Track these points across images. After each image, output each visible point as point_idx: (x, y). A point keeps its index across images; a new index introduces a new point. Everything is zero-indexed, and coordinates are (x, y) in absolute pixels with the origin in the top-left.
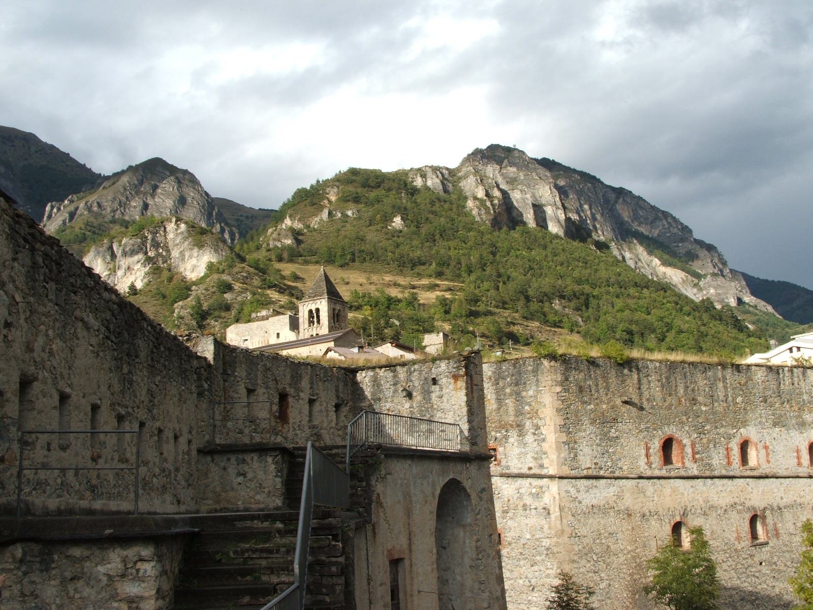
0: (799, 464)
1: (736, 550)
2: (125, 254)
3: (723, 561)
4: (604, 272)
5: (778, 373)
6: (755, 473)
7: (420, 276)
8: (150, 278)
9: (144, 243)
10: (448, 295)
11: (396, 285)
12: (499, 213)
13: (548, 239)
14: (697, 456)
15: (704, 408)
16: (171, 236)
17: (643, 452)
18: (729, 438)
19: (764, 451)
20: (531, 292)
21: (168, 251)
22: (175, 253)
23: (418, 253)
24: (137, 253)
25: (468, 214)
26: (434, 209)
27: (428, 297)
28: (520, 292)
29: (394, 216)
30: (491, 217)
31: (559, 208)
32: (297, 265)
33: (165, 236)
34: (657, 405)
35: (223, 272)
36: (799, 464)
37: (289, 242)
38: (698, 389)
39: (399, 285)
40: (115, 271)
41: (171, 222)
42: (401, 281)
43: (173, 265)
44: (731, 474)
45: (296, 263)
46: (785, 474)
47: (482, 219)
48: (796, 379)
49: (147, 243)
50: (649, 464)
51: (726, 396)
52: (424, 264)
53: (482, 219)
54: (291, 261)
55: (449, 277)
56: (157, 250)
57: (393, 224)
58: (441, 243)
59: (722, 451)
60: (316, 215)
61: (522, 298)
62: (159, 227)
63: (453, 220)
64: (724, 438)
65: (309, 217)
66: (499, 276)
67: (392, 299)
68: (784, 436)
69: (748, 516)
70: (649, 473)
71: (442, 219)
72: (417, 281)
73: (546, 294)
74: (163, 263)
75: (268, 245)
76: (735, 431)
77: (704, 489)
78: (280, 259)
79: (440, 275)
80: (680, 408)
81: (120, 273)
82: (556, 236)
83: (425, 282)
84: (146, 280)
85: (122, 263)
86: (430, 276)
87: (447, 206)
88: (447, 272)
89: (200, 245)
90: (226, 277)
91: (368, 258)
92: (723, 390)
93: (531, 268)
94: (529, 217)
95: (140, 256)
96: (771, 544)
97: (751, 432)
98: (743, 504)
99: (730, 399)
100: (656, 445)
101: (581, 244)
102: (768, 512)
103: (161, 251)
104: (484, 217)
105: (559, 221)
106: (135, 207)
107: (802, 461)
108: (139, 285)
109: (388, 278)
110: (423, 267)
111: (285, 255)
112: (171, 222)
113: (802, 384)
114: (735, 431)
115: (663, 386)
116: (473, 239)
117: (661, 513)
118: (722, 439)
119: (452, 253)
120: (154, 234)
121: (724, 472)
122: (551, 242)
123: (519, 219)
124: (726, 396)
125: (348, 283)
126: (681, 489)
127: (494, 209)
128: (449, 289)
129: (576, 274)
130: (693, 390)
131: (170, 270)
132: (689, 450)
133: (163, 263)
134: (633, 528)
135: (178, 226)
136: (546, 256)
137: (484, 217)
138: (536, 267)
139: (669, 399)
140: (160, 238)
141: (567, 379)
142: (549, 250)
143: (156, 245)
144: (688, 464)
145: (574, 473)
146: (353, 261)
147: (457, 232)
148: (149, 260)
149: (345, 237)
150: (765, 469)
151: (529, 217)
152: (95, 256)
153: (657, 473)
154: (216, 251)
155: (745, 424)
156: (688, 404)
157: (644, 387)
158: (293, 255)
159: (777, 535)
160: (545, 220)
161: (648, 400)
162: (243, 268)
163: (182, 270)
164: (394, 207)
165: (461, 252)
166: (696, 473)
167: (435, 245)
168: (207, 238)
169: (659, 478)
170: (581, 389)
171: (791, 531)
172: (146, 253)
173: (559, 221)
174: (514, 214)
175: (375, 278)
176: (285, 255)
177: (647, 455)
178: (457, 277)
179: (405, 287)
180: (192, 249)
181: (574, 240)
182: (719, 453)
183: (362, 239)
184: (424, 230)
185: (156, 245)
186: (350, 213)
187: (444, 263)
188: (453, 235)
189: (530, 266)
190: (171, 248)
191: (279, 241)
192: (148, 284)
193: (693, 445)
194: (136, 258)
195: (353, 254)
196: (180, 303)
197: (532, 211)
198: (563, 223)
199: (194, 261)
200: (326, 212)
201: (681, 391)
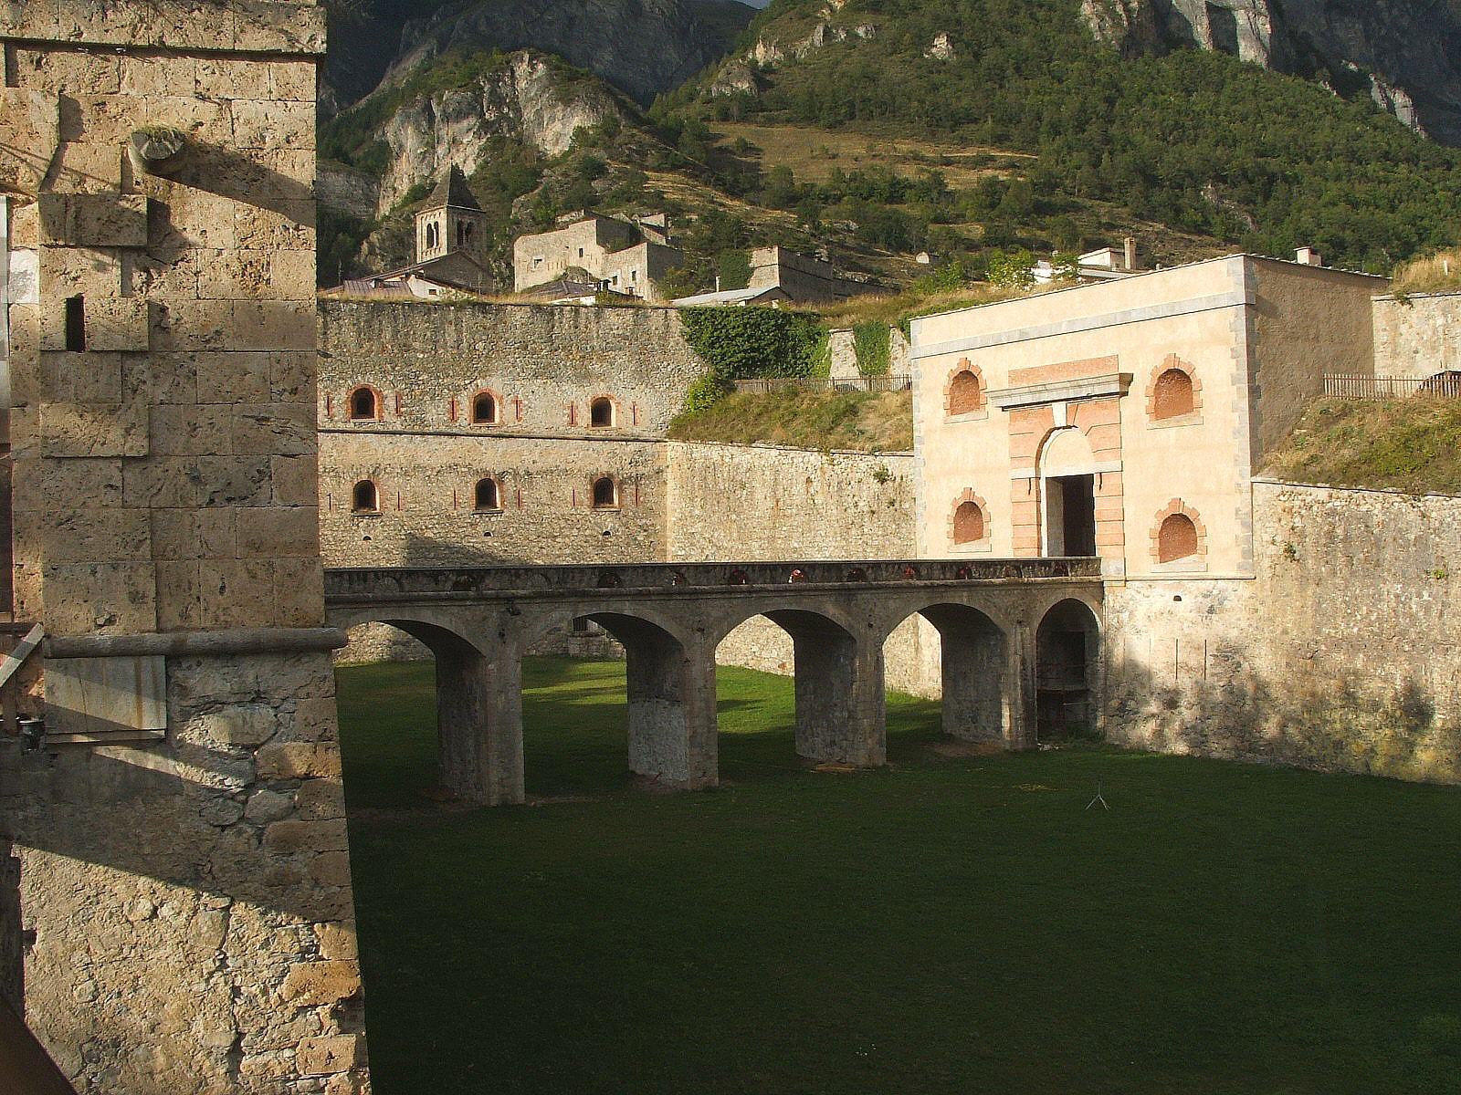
0: (572, 423)
1: (448, 517)
2: (447, 118)
3: (426, 528)
4: (1327, 131)
5: (552, 314)
6: (495, 432)
7: (964, 142)
8: (487, 157)
9: (478, 98)
10: (1003, 176)
11: (917, 158)
12: (1140, 25)
13: (1227, 73)
14: (403, 410)
16: (523, 84)
18: (457, 389)
19: (514, 406)
20: (1161, 172)
21: (518, 111)
22: (528, 114)
23: (965, 102)
24: (466, 116)
25: (1080, 29)
26: (1014, 20)
27: (961, 180)
28: (1135, 170)
29: (935, 37)
30: (1123, 33)
31: (1260, 14)
32: (753, 127)
33: (513, 85)
34: (349, 351)
35: (594, 145)
36: (572, 423)
37: (744, 86)
38: (414, 333)
39: (923, 159)
40: (433, 147)
41: (522, 61)
42: (928, 151)
43: (526, 133)
44: (454, 431)
45: (751, 122)
46: (545, 434)
47: (1105, 38)
48: (582, 321)
49: (482, 98)
50: (330, 417)
51: (459, 341)
52: (976, 121)
53: (1105, 38)
54: (743, 119)
55: (1016, 144)
56: (499, 109)
57: (934, 50)
58: (1014, 83)
59: (444, 406)
60: (806, 37)
61: (1140, 179)
62: (503, 70)
63: (1046, 40)
64: (449, 390)
65: (796, 40)
66: (1108, 140)
67: (898, 183)
68: (549, 388)
69: (473, 481)
71: (1025, 39)
72: (958, 151)
73: (1190, 174)
74: (509, 131)
75: (709, 91)
76: (467, 382)
77: (410, 446)
78: (725, 117)
79: (1000, 140)
81: (441, 150)
82: (1251, 67)
83: (971, 152)
84: (480, 161)
85: (443, 133)
86: (983, 142)
87: (1041, 14)
88: (1014, 131)
89: (567, 100)
90: (599, 154)
91: (876, 112)
93: (1177, 126)
94: (1201, 31)
95: (472, 121)
96: (506, 513)
97: (495, 385)
99: (465, 344)
101: (1301, 80)
103: (506, 110)
104: (1109, 33)
105: (1258, 38)
106: (551, 23)
107: (578, 419)
108: (469, 169)
109: (904, 147)
110: (972, 127)
111: (735, 110)
112: (522, 61)
113: (593, 326)
114: (467, 382)
116: (1076, 74)
117: (340, 470)
118: (446, 390)
119: (1029, 101)
120: (494, 82)
121: (443, 429)
122: (1234, 77)
123: (1182, 34)
124: (459, 341)
125: (834, 157)
126: (375, 445)
127: (1129, 18)
128: (1012, 165)
129: (1268, 137)
130: (407, 334)
131: (520, 142)
132: (391, 403)
133: (509, 131)
135: (533, 67)
136: (1216, 104)
137: (1109, 33)
138: (1189, 123)
139: (367, 345)
140: (504, 90)
142: (1227, 90)
143: (498, 101)
144: (386, 417)
146: (852, 116)
147: (1050, 60)
148: (485, 126)
149: (843, 75)
150: (512, 425)
151: (1201, 31)
152: (403, 122)
153: (341, 426)
154: (593, 108)
155: (484, 374)
156: (396, 351)
157: (332, 332)
158: (748, 109)
159: (519, 504)
160: (1233, 37)
161: (336, 347)
162: (633, 136)
163: (539, 141)
164: (936, 18)
165: (1047, 98)
166: (399, 428)
167: (1001, 87)
168: (578, 87)
169: (343, 432)
171: (544, 500)
172: (482, 115)
173: (1258, 38)
174: (1174, 25)
175: (881, 146)
176: (735, 110)
178: (1031, 143)
179: (933, 163)
180: (553, 106)
181: (1287, 72)
182: (439, 407)
183: (872, 79)
184: (991, 56)
185: (498, 101)
186: (861, 32)
187: (1010, 119)
188: (1040, 68)
189: (1177, 123)
190: (522, 104)
191: (727, 84)
192: (482, 167)
193: (398, 398)
194: (465, 123)
195: (852, 105)
196: (522, 198)
197: (1205, 21)
198: (1267, 41)
199: (557, 126)
200: (820, 29)
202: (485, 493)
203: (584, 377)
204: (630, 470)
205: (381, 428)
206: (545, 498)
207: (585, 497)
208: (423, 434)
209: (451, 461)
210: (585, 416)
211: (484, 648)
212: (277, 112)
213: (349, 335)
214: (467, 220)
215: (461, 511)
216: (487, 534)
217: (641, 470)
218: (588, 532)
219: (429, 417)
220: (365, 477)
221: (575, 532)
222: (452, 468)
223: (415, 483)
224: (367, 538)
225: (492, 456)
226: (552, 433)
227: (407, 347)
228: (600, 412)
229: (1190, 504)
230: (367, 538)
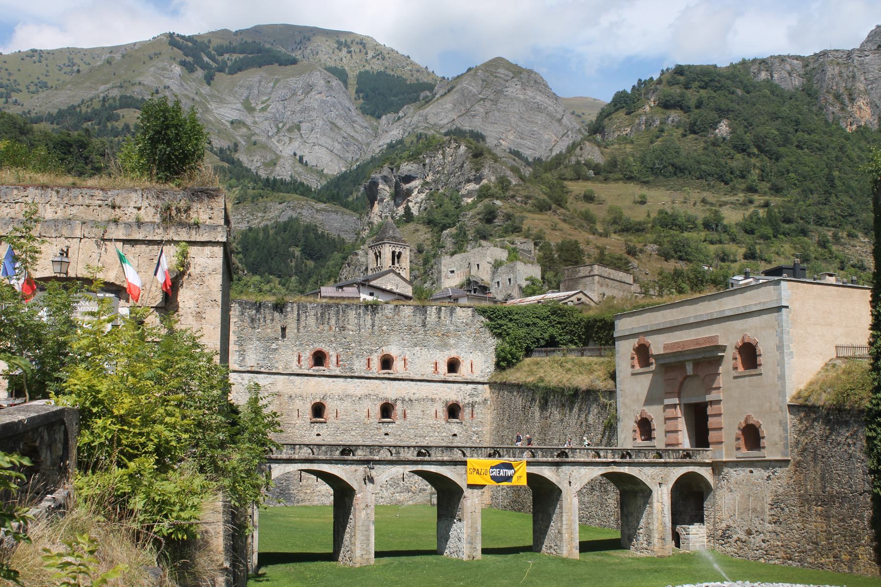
6: (391, 376)
15: (351, 333)
17: (296, 358)
18: (371, 352)
27: (732, 217)
44: (370, 375)
70: (300, 372)
80: (332, 333)
92: (370, 321)
97: (393, 351)
98: (377, 395)
100: (307, 355)
102: (399, 403)
115: (317, 319)
121: (363, 374)
124: (373, 326)
132: (334, 359)
134: (281, 404)
141: (243, 314)
145: (241, 369)
153: (306, 372)
155: (387, 343)
157: (303, 318)
166: (338, 373)
170: (253, 320)
177: (299, 361)
201: (333, 321)
202: (387, 410)
203: (445, 346)
204: (469, 400)
205: (328, 374)
206: (420, 414)
207: (442, 413)
208: (352, 377)
209: (367, 393)
210: (443, 368)
211: (355, 486)
212: (210, 261)
213: (312, 321)
214: (397, 250)
215: (372, 421)
216: (386, 434)
217: (476, 399)
218: (445, 434)
219: (355, 368)
220: (318, 400)
221: (436, 434)
222: (367, 396)
223: (347, 404)
224: (318, 435)
225: (390, 391)
226: (425, 378)
227: (343, 328)
228: (453, 366)
229: (755, 419)
230: (318, 435)
